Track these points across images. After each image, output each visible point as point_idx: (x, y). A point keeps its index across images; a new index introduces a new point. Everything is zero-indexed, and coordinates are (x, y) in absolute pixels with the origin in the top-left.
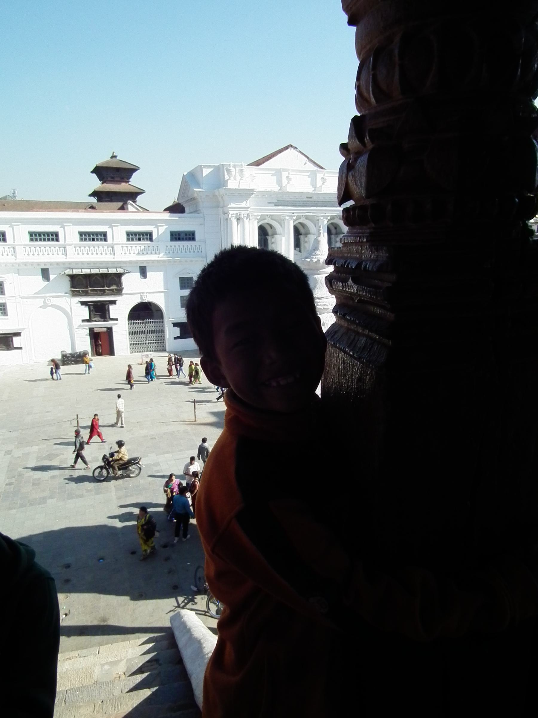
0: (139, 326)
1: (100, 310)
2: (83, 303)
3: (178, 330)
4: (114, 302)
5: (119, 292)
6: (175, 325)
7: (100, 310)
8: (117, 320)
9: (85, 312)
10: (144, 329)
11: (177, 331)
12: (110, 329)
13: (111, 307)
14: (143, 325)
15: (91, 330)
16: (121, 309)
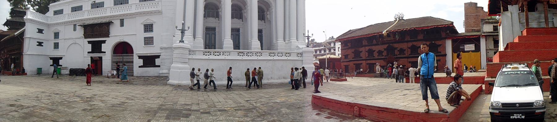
0: (118, 57)
1: (96, 47)
2: (89, 42)
3: (142, 60)
4: (104, 42)
5: (107, 35)
6: (140, 57)
7: (96, 47)
8: (105, 52)
9: (89, 47)
10: (121, 60)
11: (141, 62)
12: (101, 58)
13: (103, 45)
14: (121, 57)
15: (91, 57)
16: (108, 47)
